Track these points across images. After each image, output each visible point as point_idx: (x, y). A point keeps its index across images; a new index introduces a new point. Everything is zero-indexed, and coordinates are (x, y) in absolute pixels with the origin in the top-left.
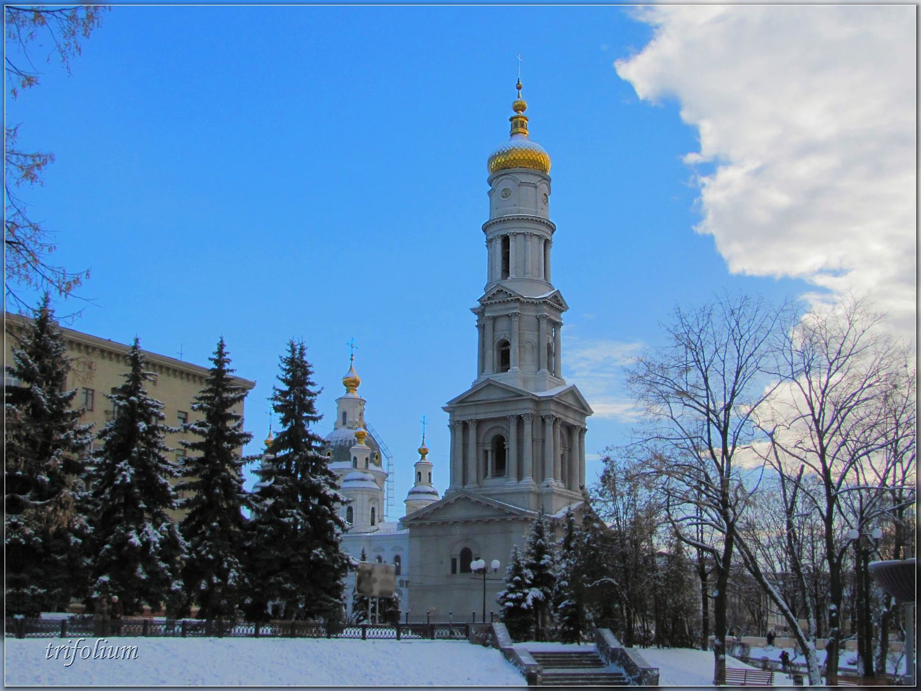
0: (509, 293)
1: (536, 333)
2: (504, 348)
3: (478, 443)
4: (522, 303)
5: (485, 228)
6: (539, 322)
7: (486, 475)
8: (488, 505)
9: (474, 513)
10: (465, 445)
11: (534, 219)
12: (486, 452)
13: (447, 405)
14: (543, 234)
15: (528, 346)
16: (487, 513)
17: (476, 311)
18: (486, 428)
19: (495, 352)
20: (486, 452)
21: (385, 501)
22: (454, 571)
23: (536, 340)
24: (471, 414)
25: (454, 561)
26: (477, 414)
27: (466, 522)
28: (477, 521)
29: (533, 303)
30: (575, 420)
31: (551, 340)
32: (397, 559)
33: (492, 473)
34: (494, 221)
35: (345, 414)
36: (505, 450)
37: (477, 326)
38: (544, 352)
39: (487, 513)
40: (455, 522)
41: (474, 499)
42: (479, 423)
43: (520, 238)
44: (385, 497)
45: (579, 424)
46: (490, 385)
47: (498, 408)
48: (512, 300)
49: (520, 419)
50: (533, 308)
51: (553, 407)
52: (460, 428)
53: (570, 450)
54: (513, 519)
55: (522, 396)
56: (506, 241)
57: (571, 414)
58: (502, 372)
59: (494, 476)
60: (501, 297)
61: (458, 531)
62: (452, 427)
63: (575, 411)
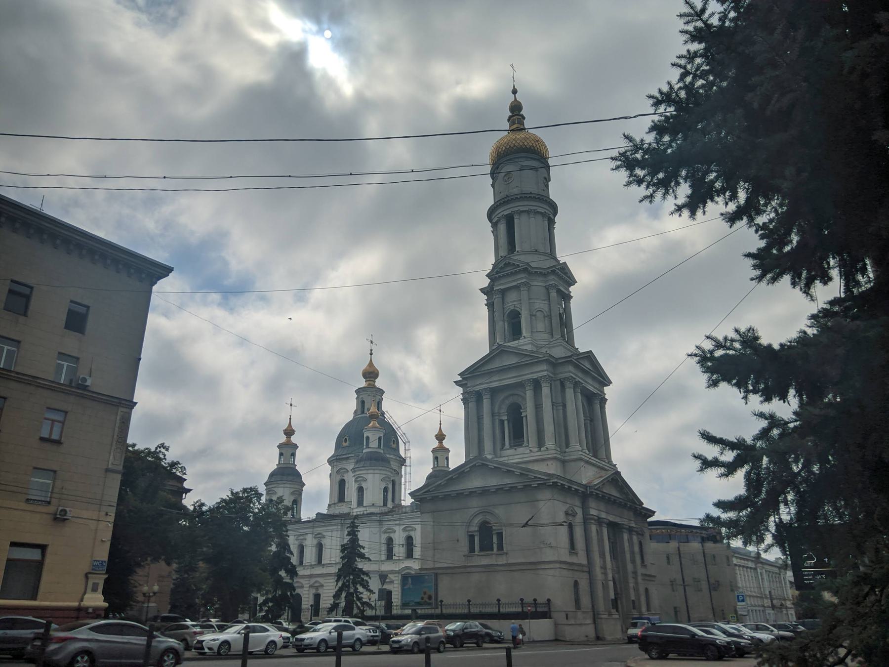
3: (493, 415)
4: (530, 273)
5: (491, 214)
7: (503, 445)
8: (509, 471)
9: (493, 481)
10: (480, 419)
11: (537, 197)
12: (502, 422)
13: (459, 378)
15: (539, 314)
16: (507, 481)
18: (501, 397)
19: (506, 323)
20: (502, 422)
21: (403, 486)
22: (472, 550)
23: (546, 308)
24: (482, 384)
25: (471, 538)
26: (491, 382)
27: (484, 492)
28: (498, 489)
29: (541, 273)
30: (594, 387)
31: (562, 311)
32: (409, 541)
33: (510, 443)
34: (498, 203)
35: (363, 403)
36: (523, 417)
37: (486, 305)
38: (556, 320)
40: (471, 492)
41: (492, 465)
42: (494, 392)
43: (524, 217)
44: (403, 481)
45: (599, 392)
46: (503, 351)
49: (537, 385)
51: (571, 368)
52: (473, 399)
53: (592, 420)
54: (538, 484)
57: (590, 381)
58: (513, 341)
59: (511, 447)
60: (509, 270)
61: (475, 504)
63: (594, 378)
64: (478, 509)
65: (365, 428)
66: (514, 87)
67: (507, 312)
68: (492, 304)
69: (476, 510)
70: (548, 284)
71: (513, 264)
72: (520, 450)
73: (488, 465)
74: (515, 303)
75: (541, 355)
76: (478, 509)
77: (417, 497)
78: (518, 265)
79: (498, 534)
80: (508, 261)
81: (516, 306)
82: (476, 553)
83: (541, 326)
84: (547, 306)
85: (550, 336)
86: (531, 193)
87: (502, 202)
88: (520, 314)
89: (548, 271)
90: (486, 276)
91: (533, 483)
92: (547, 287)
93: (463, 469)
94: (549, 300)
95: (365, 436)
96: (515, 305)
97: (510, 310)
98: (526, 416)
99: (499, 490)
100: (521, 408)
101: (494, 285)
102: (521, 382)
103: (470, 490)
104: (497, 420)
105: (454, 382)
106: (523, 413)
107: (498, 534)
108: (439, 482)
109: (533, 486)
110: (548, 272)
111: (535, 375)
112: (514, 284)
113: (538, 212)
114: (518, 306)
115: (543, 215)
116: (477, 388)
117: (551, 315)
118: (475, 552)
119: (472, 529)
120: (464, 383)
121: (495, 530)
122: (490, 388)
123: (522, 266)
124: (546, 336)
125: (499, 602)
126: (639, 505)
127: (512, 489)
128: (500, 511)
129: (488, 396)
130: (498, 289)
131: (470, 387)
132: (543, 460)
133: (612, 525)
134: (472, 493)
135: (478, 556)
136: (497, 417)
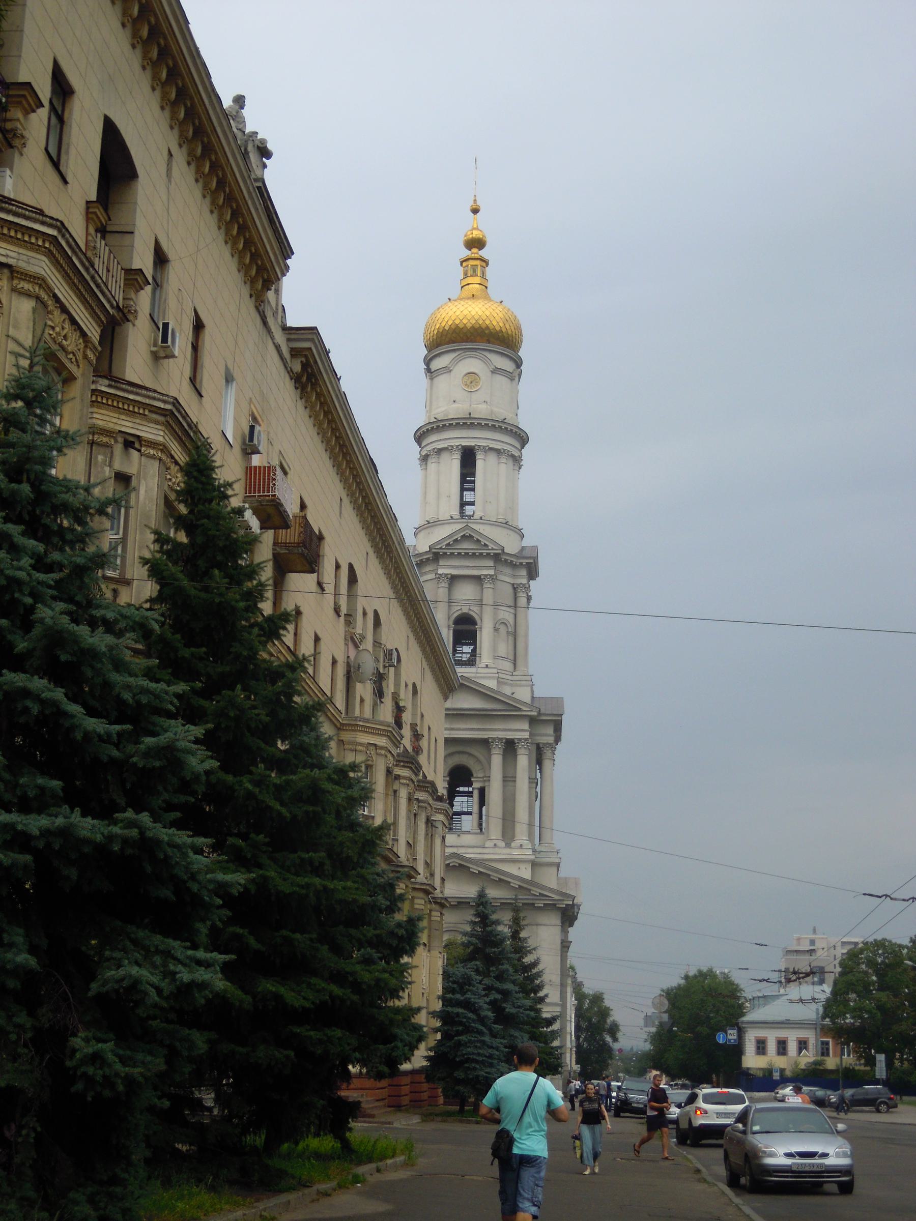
0: (483, 541)
2: (460, 627)
6: (515, 594)
15: (503, 629)
23: (511, 620)
41: (475, 869)
43: (492, 458)
48: (488, 554)
49: (510, 747)
50: (508, 570)
54: (544, 904)
56: (468, 458)
60: (467, 546)
66: (475, 200)
73: (469, 868)
78: (485, 545)
83: (504, 649)
84: (512, 616)
85: (512, 665)
89: (521, 561)
91: (537, 902)
94: (515, 607)
97: (459, 612)
109: (536, 905)
110: (521, 563)
117: (515, 632)
123: (493, 549)
124: (508, 666)
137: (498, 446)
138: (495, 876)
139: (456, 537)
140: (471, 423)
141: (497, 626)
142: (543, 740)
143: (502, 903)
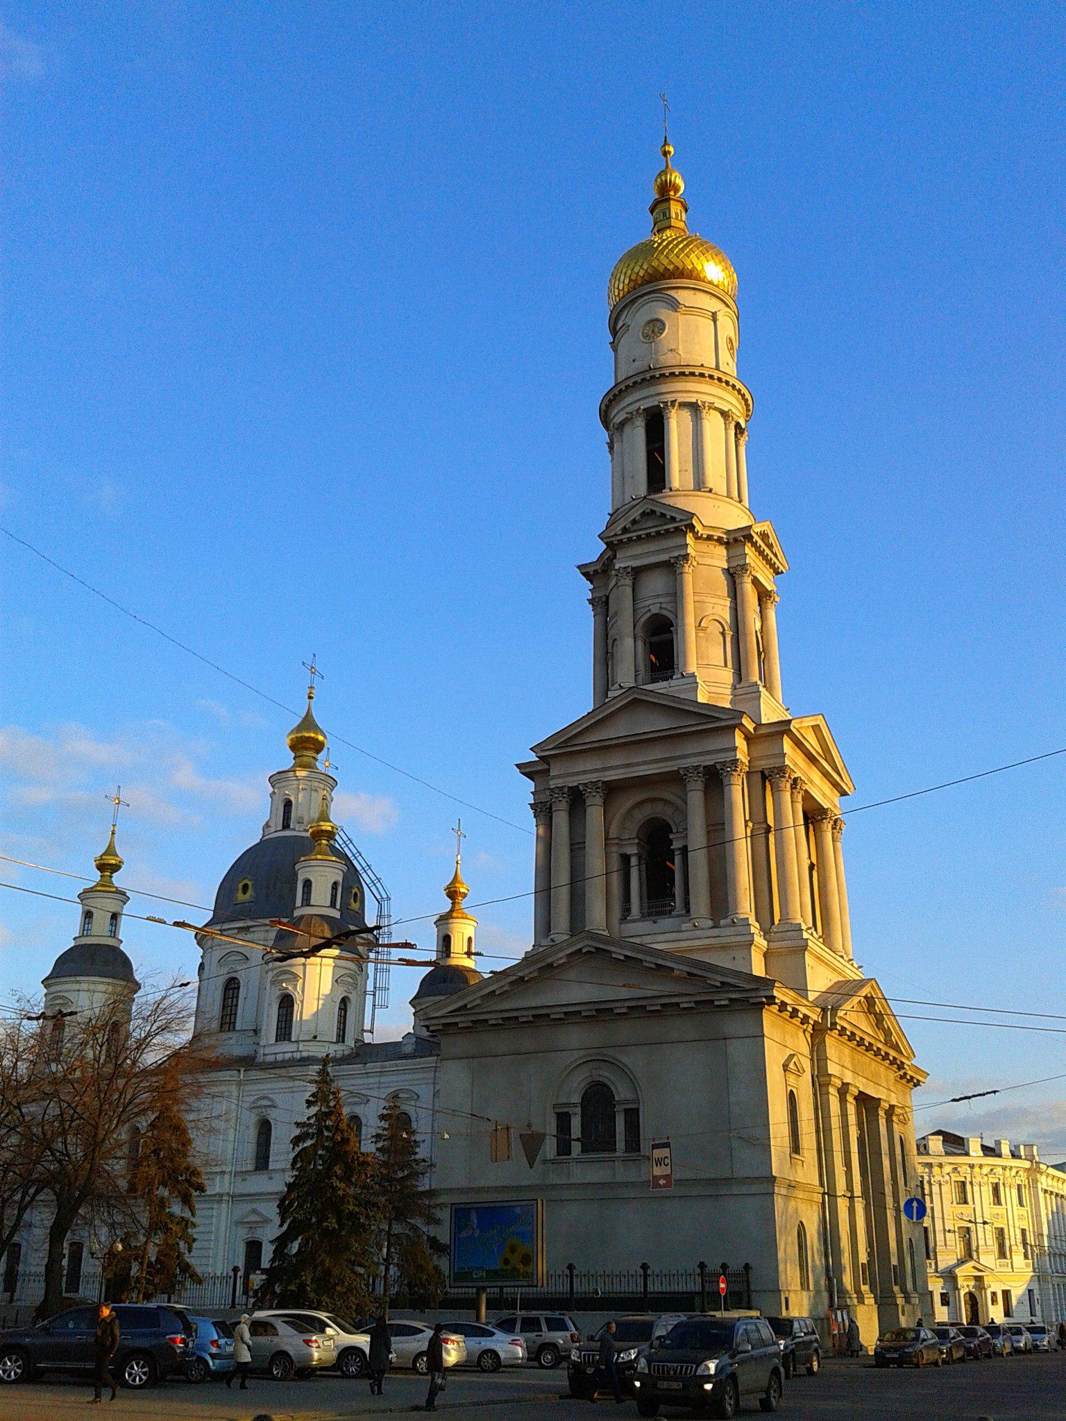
0: (669, 514)
1: (728, 602)
2: (654, 639)
4: (698, 537)
6: (735, 582)
7: (626, 910)
9: (616, 990)
12: (625, 859)
14: (734, 410)
16: (654, 988)
17: (591, 570)
18: (626, 803)
19: (640, 644)
23: (726, 616)
25: (563, 1120)
26: (605, 769)
27: (601, 1013)
30: (824, 795)
33: (641, 908)
36: (673, 851)
39: (654, 988)
41: (619, 953)
42: (611, 790)
47: (657, 753)
48: (677, 529)
55: (721, 720)
60: (651, 526)
61: (576, 1039)
62: (543, 810)
64: (582, 1053)
65: (302, 859)
67: (643, 620)
68: (604, 599)
69: (576, 1054)
70: (735, 564)
71: (661, 513)
72: (666, 923)
73: (610, 952)
74: (661, 600)
75: (729, 714)
76: (582, 1053)
77: (434, 1022)
78: (673, 519)
79: (626, 1111)
80: (651, 507)
81: (663, 606)
82: (574, 1155)
86: (702, 366)
87: (638, 379)
88: (672, 626)
90: (599, 536)
92: (731, 571)
93: (550, 960)
95: (301, 878)
96: (661, 603)
97: (649, 614)
98: (685, 851)
99: (638, 1010)
100: (672, 832)
101: (615, 557)
102: (678, 771)
103: (565, 1010)
104: (615, 855)
105: (518, 766)
106: (674, 843)
107: (626, 1111)
108: (491, 989)
109: (717, 1003)
111: (708, 757)
112: (663, 557)
113: (716, 409)
114: (669, 607)
115: (724, 414)
116: (572, 782)
118: (570, 1154)
119: (563, 1100)
120: (539, 768)
121: (620, 1102)
122: (603, 782)
125: (645, 1272)
126: (908, 1058)
127: (669, 1009)
128: (633, 1060)
129: (598, 800)
130: (625, 568)
131: (559, 776)
132: (724, 948)
133: (864, 1100)
134: (572, 1016)
135: (578, 1161)
136: (614, 849)
137: (692, 398)
138: (650, 961)
139: (632, 518)
140: (651, 377)
141: (702, 625)
142: (764, 764)
143: (662, 1005)
